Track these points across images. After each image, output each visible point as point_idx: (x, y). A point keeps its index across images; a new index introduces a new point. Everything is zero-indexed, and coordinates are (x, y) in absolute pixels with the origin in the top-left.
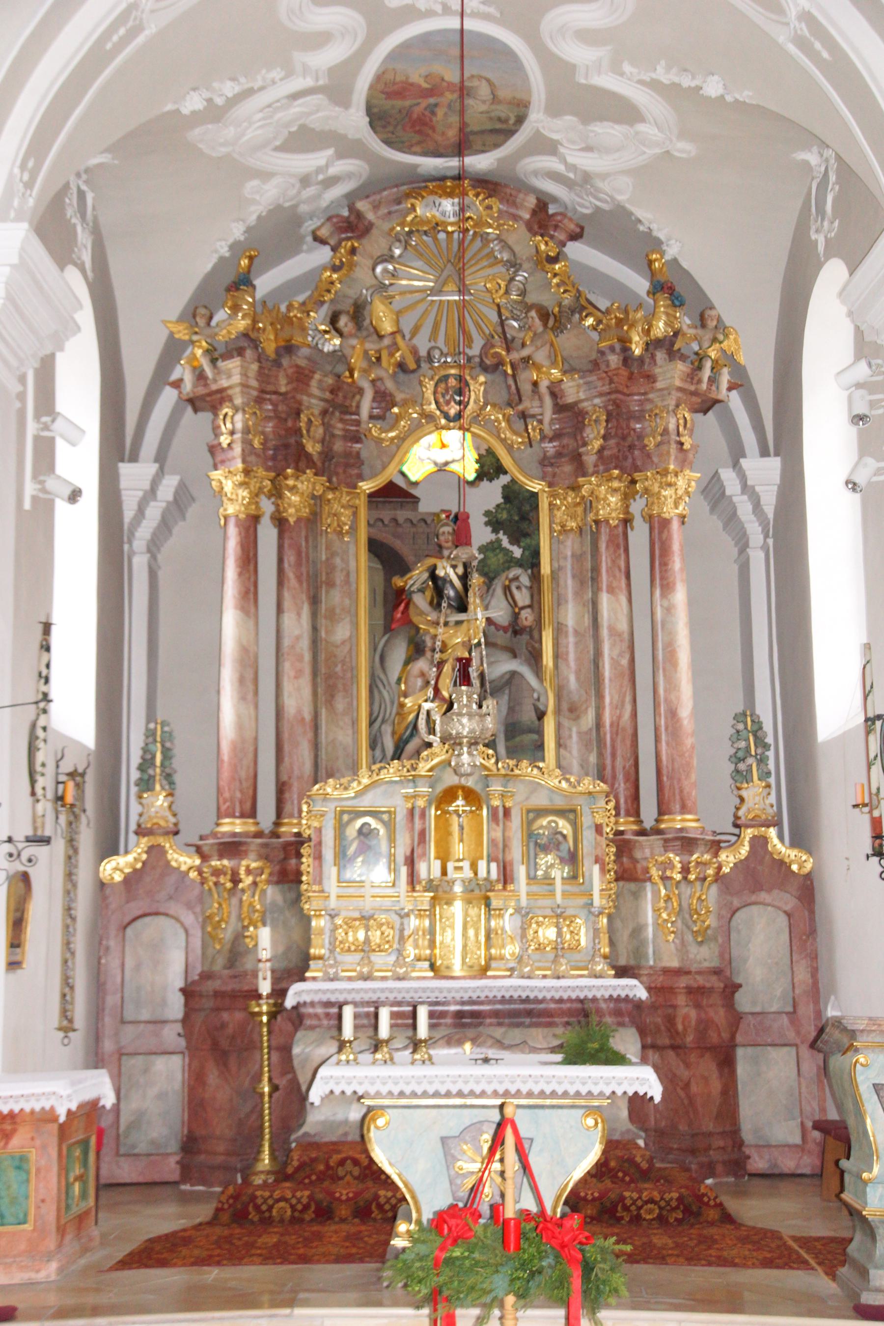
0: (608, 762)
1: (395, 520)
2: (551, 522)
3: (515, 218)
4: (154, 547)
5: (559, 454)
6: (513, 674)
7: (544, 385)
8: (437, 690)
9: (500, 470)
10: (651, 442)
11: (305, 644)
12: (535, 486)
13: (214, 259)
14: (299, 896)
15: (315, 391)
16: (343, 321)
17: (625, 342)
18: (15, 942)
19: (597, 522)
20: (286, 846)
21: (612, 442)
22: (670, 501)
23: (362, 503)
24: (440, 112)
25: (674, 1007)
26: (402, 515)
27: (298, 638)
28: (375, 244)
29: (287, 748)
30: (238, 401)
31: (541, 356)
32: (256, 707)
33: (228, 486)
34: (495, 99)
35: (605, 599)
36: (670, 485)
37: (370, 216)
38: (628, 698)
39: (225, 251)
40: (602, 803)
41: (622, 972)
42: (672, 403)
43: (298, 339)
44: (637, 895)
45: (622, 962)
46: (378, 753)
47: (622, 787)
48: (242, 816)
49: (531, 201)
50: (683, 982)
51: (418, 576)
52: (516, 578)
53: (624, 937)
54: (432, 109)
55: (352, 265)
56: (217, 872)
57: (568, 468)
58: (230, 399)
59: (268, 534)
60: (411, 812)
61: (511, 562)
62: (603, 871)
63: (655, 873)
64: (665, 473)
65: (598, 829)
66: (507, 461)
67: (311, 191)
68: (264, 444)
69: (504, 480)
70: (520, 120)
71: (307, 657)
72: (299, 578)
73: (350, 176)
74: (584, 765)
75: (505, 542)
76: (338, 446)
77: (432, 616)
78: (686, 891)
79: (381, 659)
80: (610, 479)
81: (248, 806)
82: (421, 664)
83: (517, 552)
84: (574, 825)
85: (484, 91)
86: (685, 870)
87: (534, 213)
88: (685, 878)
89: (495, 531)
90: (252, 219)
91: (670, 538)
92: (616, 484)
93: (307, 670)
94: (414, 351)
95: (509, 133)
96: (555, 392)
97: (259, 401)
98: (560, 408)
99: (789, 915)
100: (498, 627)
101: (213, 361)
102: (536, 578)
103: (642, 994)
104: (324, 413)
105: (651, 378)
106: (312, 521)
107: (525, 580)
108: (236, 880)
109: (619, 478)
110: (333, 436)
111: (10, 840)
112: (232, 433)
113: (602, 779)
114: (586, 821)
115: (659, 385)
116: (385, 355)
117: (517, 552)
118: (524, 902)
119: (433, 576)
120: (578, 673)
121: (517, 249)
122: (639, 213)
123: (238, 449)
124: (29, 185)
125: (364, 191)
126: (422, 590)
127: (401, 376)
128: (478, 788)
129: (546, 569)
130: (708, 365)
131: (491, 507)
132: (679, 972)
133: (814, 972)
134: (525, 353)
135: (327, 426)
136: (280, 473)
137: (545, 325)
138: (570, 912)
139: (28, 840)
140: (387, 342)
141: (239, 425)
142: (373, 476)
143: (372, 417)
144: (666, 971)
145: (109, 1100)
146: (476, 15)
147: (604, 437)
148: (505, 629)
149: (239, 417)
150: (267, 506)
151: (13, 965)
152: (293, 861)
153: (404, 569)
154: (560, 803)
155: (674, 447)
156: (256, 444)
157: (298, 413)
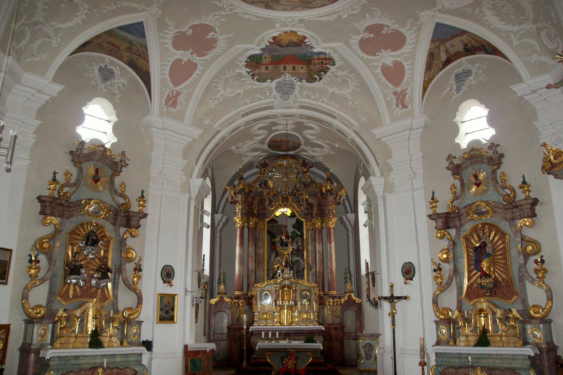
0: (318, 279)
1: (273, 226)
2: (306, 228)
3: (298, 163)
4: (221, 231)
5: (308, 213)
6: (298, 260)
7: (304, 199)
8: (282, 264)
9: (295, 216)
10: (327, 212)
11: (253, 254)
12: (303, 220)
13: (236, 172)
14: (252, 308)
15: (256, 200)
16: (262, 185)
17: (321, 190)
18: (196, 318)
19: (316, 228)
20: (249, 297)
21: (319, 212)
22: (331, 224)
23: (266, 223)
24: (283, 145)
25: (331, 331)
26: (274, 225)
27: (252, 253)
28: (269, 168)
29: (249, 276)
30: (240, 203)
31: (304, 193)
32: (243, 267)
33: (238, 220)
34: (294, 143)
35: (317, 245)
36: (331, 221)
37: (268, 163)
38: (322, 266)
39: (238, 170)
40: (316, 289)
41: (320, 324)
42: (331, 204)
43: (253, 189)
44: (323, 308)
45: (320, 322)
46: (269, 277)
47: (321, 285)
48: (240, 291)
49: (302, 160)
50: (333, 326)
51: (278, 239)
52: (299, 240)
53: (320, 317)
54: (281, 145)
55: (264, 173)
56: (235, 303)
57: (309, 216)
58: (239, 203)
59: (246, 230)
60: (276, 290)
61: (298, 236)
62: (316, 303)
63: (327, 303)
64: (330, 218)
65: (315, 294)
66: (297, 214)
67: (256, 158)
68: (245, 212)
69: (296, 218)
70: (299, 146)
71: (254, 257)
72: (252, 240)
73: (264, 155)
74: (313, 280)
75: (296, 231)
76: (261, 211)
77: (281, 248)
78: (334, 307)
79: (269, 257)
80: (318, 219)
81: (241, 288)
82: (278, 258)
83: (299, 233)
84: (310, 293)
85: (292, 142)
86: (333, 303)
87: (302, 162)
88: (333, 304)
89: (294, 229)
90: (244, 164)
91: (331, 232)
92: (319, 220)
93: (254, 260)
94: (277, 191)
95: (297, 148)
96: (307, 200)
97: (244, 203)
98: (307, 204)
99: (355, 311)
100: (295, 250)
101: (235, 195)
102: (303, 239)
103: (324, 329)
104: (258, 204)
105: (326, 199)
106: (255, 228)
107: (300, 240)
108: (239, 304)
109: (320, 219)
110: (260, 209)
111: (196, 298)
112: (239, 209)
113: (316, 283)
114: (313, 292)
115: (328, 200)
116: (271, 192)
117: (299, 233)
118: (299, 310)
119: (281, 239)
120: (311, 260)
121: (299, 170)
122: (324, 163)
123: (240, 213)
124: (203, 169)
125: (267, 158)
126: (278, 242)
127: (274, 196)
128: (290, 285)
129: (305, 237)
130: (338, 196)
131: (294, 224)
132: (332, 324)
133: (361, 324)
134: (300, 192)
135: (258, 207)
136: (249, 218)
137: (305, 186)
138: (309, 312)
139: (200, 298)
140: (271, 189)
141: (240, 208)
142: (268, 218)
143: (268, 205)
144: (329, 324)
145: (215, 349)
146: (289, 131)
147: (317, 210)
148: (296, 251)
149: (240, 206)
150: (246, 225)
151: (196, 322)
152: (251, 301)
153: (275, 237)
154: (307, 288)
155: (331, 213)
156: (244, 211)
157: (253, 205)
